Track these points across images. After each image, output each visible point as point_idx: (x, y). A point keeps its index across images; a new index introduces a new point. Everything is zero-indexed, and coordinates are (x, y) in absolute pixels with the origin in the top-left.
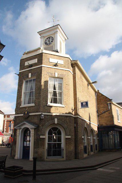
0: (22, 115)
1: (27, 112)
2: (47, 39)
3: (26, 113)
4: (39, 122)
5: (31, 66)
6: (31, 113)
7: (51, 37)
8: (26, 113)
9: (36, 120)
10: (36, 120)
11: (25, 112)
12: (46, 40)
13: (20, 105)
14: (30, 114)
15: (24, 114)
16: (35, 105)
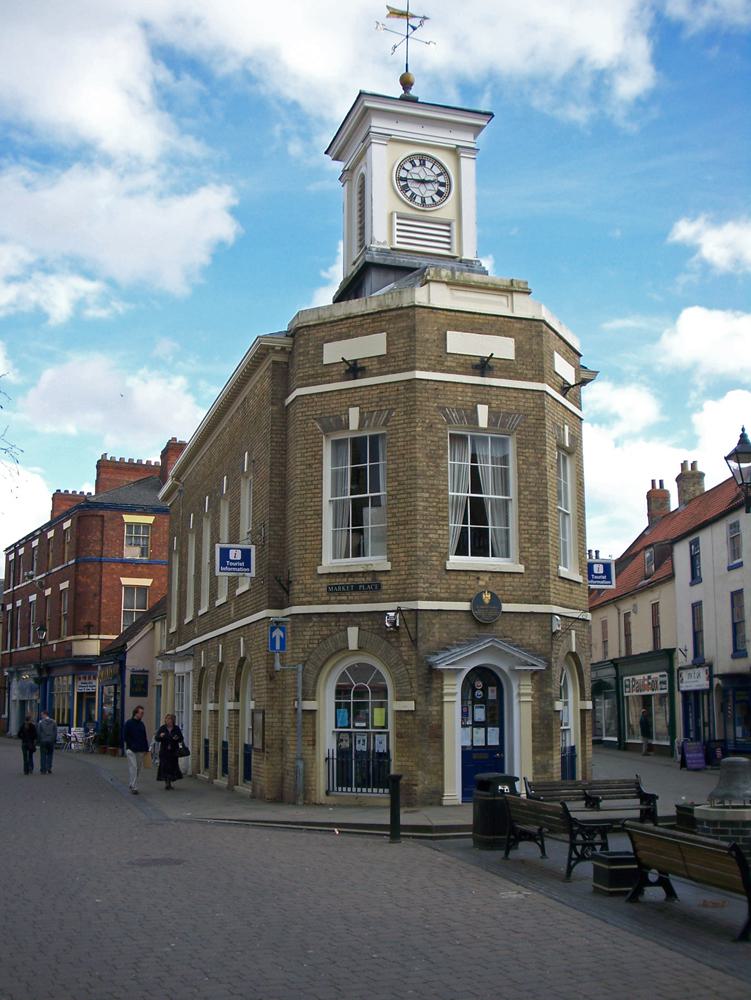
0: (465, 606)
1: (493, 595)
2: (411, 159)
3: (487, 597)
4: (550, 646)
5: (483, 366)
6: (508, 602)
7: (436, 162)
8: (487, 597)
9: (532, 635)
10: (532, 637)
11: (479, 596)
12: (401, 167)
13: (445, 557)
14: (506, 607)
15: (477, 601)
16: (526, 568)
